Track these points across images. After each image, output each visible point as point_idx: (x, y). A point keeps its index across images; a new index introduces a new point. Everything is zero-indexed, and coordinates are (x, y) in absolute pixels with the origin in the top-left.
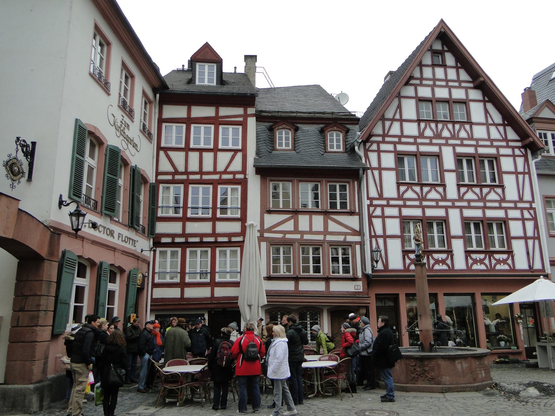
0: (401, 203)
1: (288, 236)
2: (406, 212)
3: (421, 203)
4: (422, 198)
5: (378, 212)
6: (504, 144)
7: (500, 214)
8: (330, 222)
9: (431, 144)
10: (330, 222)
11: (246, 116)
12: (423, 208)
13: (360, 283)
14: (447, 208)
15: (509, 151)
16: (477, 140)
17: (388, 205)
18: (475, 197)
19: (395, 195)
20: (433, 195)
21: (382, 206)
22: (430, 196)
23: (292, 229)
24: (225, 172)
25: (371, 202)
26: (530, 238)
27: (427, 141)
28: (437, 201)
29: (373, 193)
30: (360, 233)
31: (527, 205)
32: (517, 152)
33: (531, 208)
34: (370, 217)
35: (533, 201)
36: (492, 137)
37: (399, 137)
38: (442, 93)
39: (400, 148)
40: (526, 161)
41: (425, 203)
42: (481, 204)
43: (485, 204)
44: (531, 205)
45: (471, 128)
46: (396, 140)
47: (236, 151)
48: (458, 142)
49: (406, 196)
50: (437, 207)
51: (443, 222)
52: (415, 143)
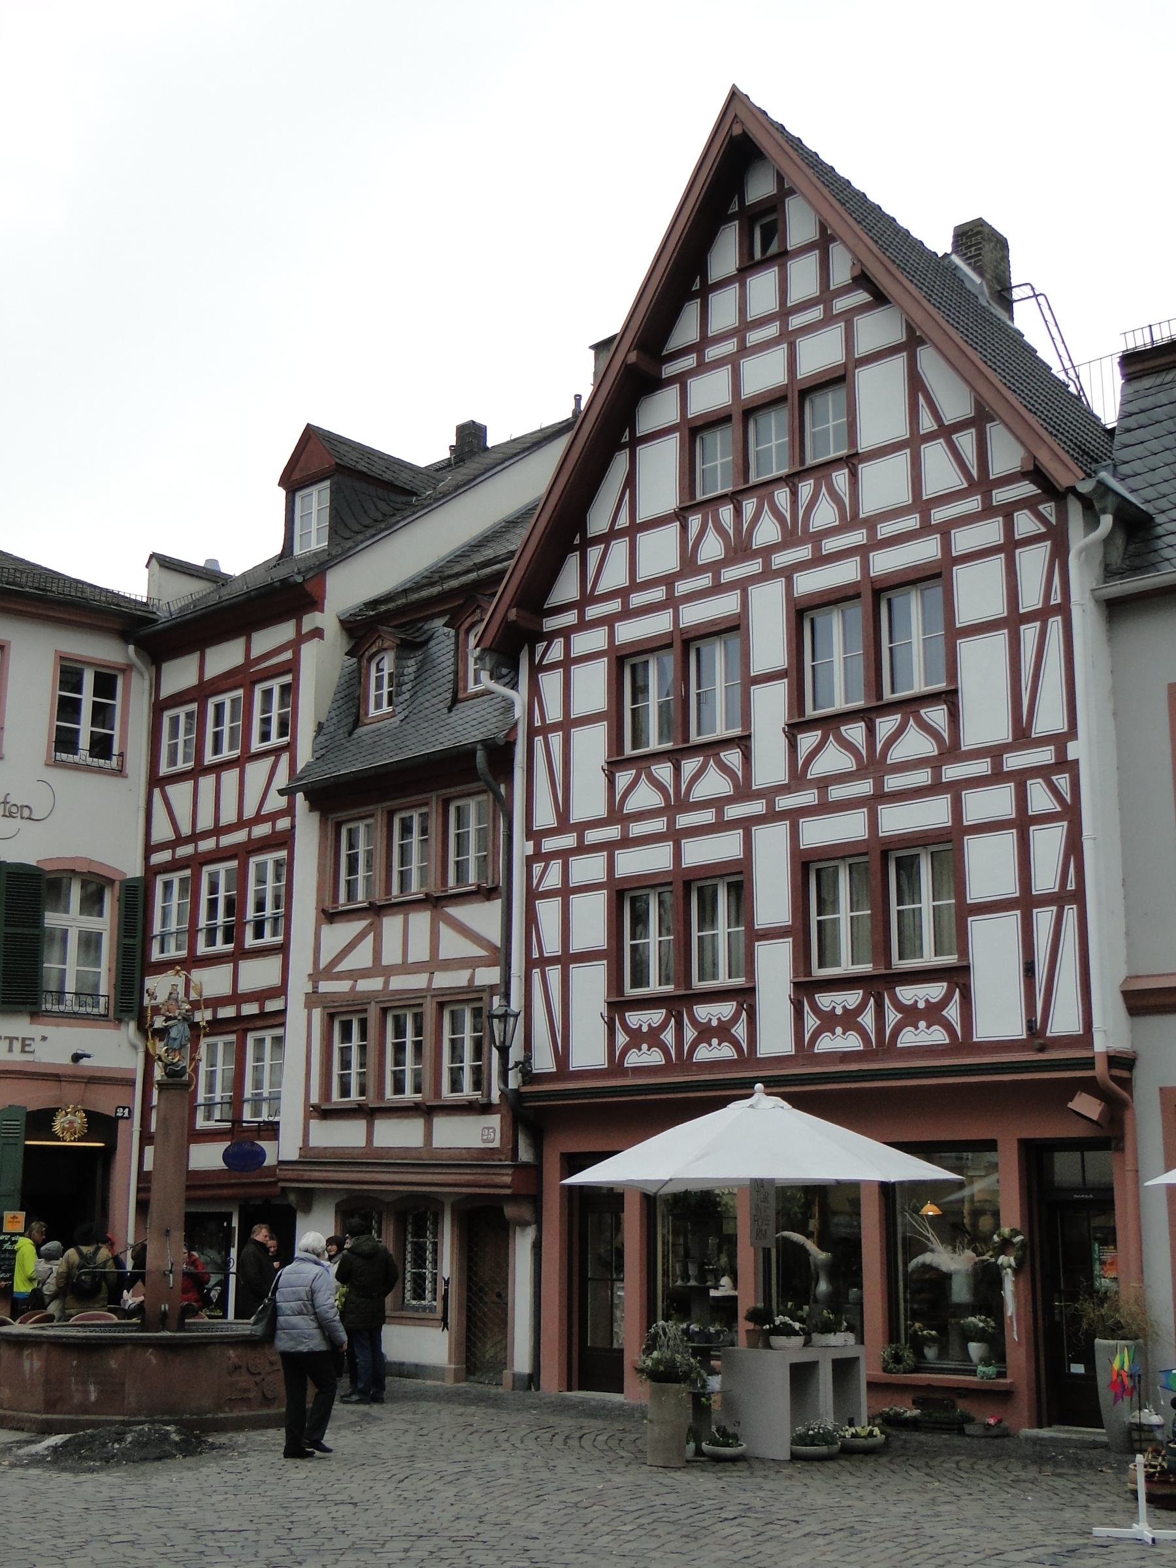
0: (612, 833)
1: (364, 985)
2: (631, 863)
3: (671, 822)
4: (677, 803)
5: (553, 879)
6: (973, 504)
7: (932, 814)
8: (445, 930)
9: (718, 588)
10: (445, 930)
11: (294, 646)
12: (675, 836)
13: (494, 1121)
14: (746, 824)
15: (990, 532)
16: (871, 523)
17: (582, 849)
18: (846, 763)
19: (600, 809)
20: (714, 784)
21: (564, 855)
22: (701, 791)
23: (369, 963)
24: (259, 819)
25: (538, 846)
26: (1046, 900)
27: (705, 581)
28: (717, 804)
29: (545, 817)
30: (501, 956)
31: (1045, 756)
32: (1025, 524)
33: (1065, 765)
34: (533, 895)
35: (1072, 732)
36: (931, 489)
37: (622, 593)
38: (764, 373)
39: (629, 632)
40: (1060, 552)
41: (685, 820)
42: (864, 787)
43: (879, 783)
44: (1061, 751)
45: (854, 475)
46: (614, 606)
47: (276, 752)
48: (804, 553)
49: (631, 805)
50: (721, 826)
51: (738, 879)
52: (672, 603)
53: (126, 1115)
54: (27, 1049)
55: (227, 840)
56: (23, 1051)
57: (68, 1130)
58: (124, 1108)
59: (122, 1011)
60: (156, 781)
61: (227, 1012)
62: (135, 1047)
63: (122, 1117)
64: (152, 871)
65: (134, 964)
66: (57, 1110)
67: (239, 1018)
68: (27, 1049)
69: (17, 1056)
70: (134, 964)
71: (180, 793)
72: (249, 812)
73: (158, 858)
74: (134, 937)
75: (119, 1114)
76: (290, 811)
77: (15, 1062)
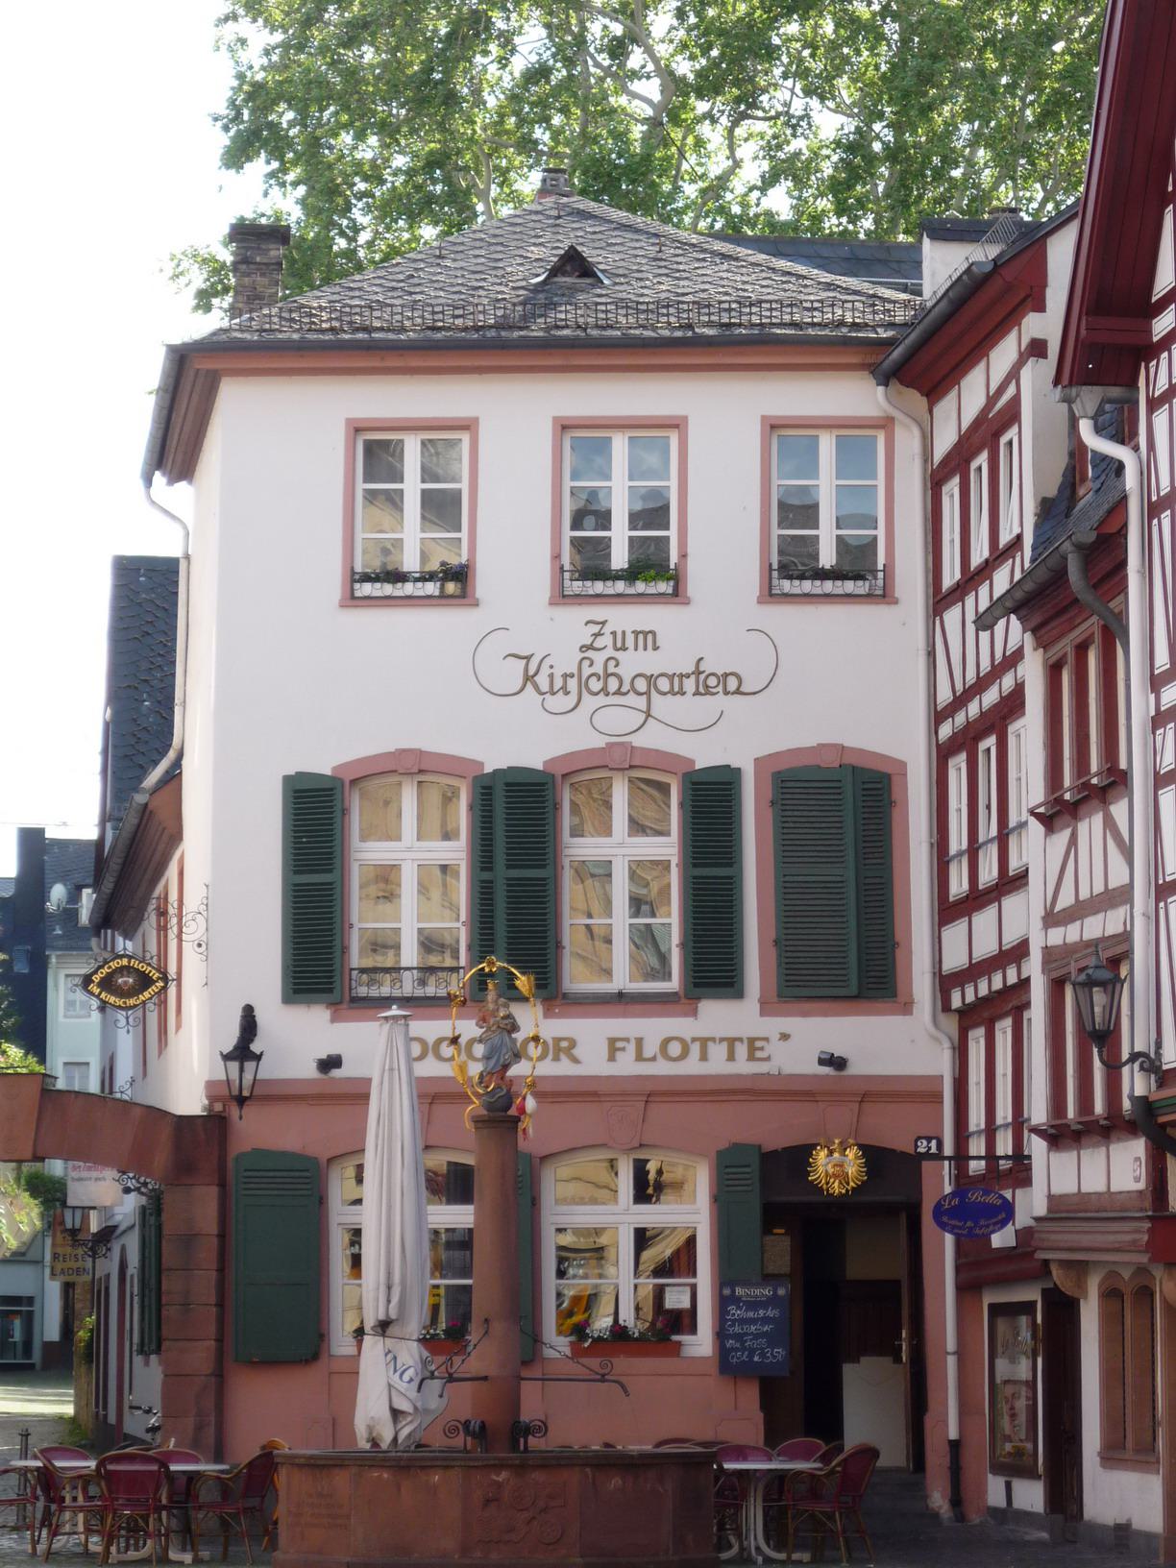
53: (934, 1150)
54: (759, 1054)
57: (835, 1176)
58: (929, 1139)
62: (936, 1039)
63: (928, 1156)
66: (813, 1146)
68: (759, 1054)
69: (743, 1066)
75: (922, 1150)
77: (739, 1076)
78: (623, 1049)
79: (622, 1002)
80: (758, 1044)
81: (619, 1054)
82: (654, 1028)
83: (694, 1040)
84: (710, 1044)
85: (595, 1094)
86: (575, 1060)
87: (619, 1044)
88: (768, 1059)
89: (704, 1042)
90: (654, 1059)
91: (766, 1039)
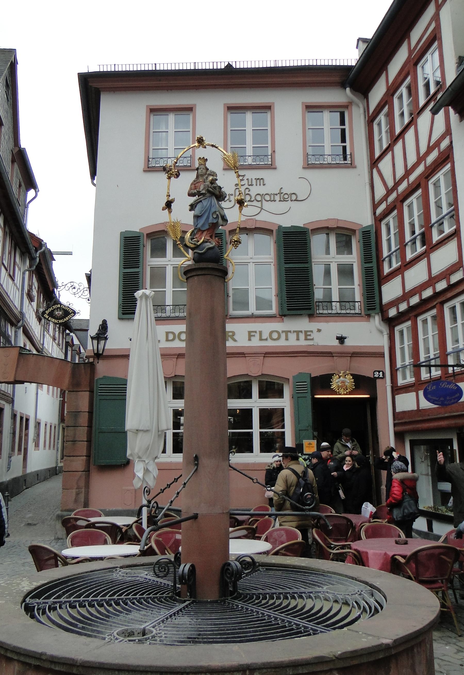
53: (381, 376)
54: (309, 337)
55: (412, 178)
56: (306, 339)
58: (379, 372)
59: (369, 310)
60: (374, 163)
61: (428, 293)
62: (381, 332)
63: (379, 378)
64: (378, 220)
65: (374, 280)
66: (333, 375)
67: (436, 295)
68: (309, 337)
69: (303, 343)
70: (374, 280)
71: (385, 165)
72: (423, 149)
73: (379, 210)
74: (371, 262)
75: (376, 376)
76: (448, 132)
78: (254, 336)
79: (253, 317)
80: (308, 333)
81: (252, 338)
82: (266, 327)
83: (283, 332)
84: (289, 334)
85: (243, 354)
86: (235, 341)
87: (252, 334)
88: (313, 339)
89: (287, 332)
90: (266, 339)
91: (312, 331)
